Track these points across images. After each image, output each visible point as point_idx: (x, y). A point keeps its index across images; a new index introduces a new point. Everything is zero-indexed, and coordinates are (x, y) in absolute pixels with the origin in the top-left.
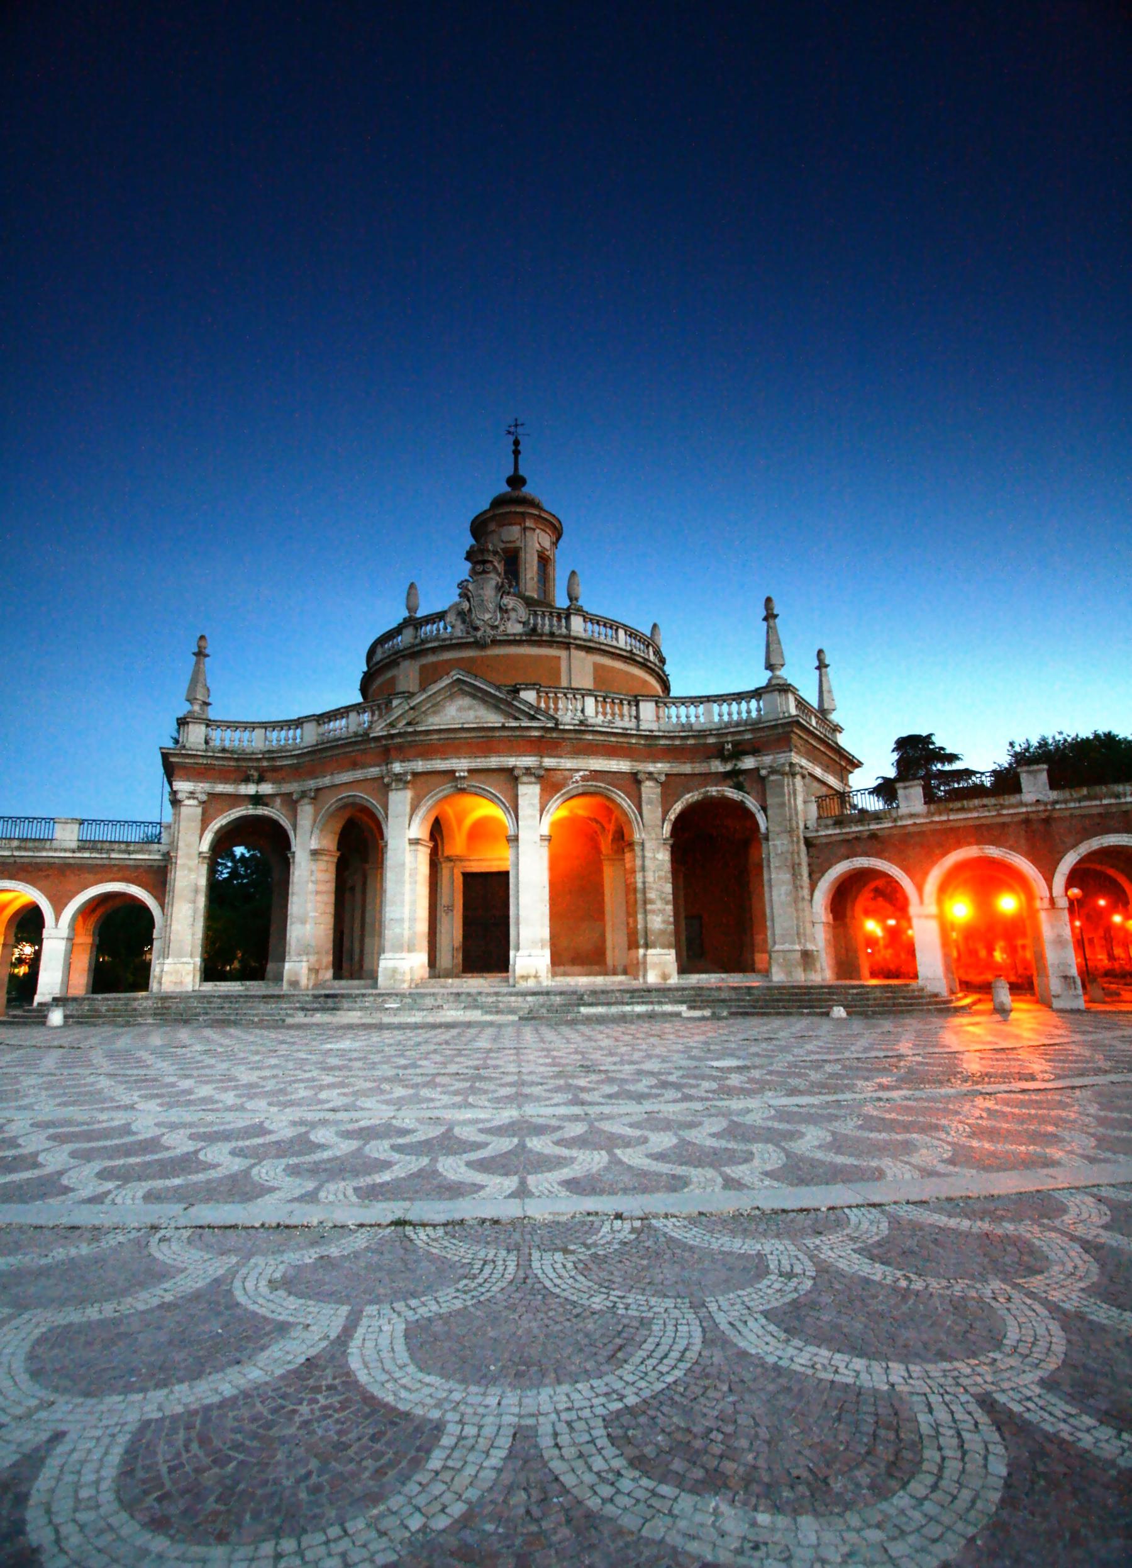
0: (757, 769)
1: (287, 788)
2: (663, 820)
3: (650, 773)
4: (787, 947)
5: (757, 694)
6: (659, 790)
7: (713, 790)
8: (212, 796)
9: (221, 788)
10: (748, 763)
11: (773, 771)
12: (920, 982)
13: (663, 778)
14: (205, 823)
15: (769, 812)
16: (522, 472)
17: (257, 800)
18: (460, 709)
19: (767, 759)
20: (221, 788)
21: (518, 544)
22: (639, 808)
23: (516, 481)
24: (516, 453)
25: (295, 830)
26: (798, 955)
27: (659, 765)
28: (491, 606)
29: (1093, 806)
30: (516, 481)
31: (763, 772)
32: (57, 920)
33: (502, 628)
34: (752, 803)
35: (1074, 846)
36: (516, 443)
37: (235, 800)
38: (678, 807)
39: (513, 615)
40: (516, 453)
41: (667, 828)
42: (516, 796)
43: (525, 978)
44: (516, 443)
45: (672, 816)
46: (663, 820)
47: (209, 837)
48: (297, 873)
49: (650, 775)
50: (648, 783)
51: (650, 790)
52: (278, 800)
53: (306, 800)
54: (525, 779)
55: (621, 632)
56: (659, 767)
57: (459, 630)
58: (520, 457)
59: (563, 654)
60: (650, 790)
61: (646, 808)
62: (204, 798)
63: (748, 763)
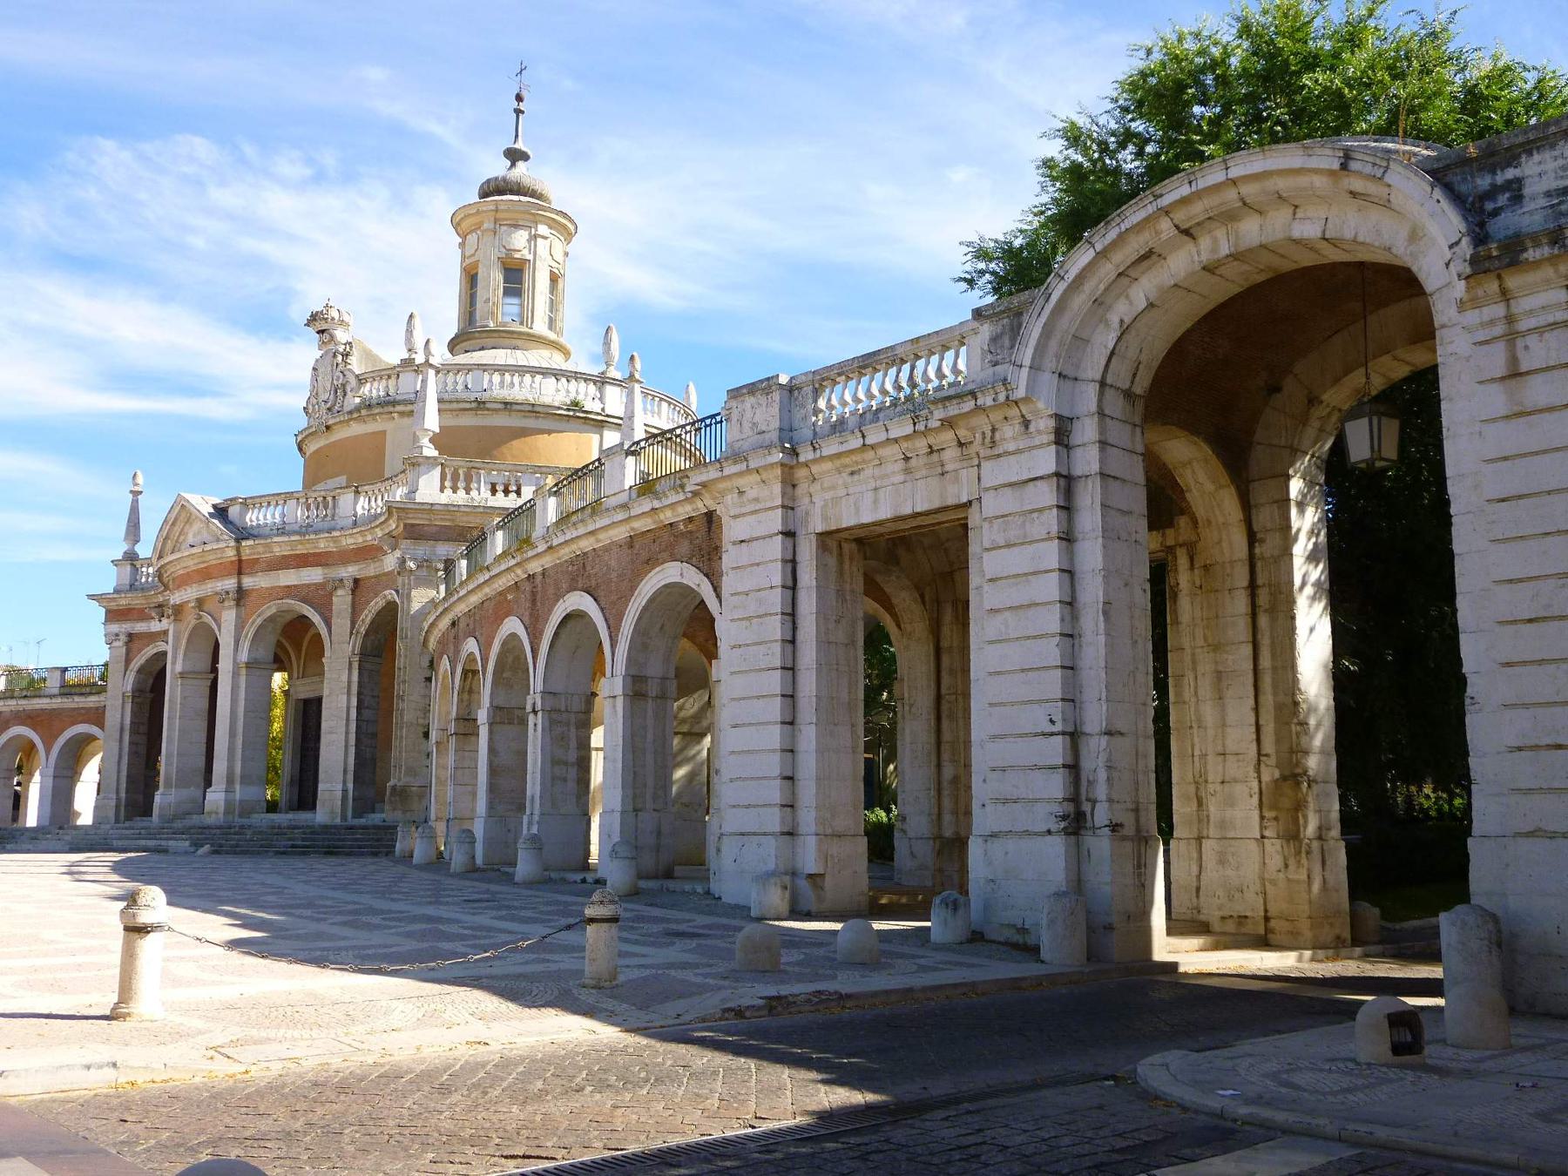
8: (130, 636)
14: (128, 661)
24: (518, 112)
27: (350, 569)
36: (519, 98)
38: (367, 616)
47: (131, 677)
50: (340, 592)
56: (349, 571)
62: (123, 638)
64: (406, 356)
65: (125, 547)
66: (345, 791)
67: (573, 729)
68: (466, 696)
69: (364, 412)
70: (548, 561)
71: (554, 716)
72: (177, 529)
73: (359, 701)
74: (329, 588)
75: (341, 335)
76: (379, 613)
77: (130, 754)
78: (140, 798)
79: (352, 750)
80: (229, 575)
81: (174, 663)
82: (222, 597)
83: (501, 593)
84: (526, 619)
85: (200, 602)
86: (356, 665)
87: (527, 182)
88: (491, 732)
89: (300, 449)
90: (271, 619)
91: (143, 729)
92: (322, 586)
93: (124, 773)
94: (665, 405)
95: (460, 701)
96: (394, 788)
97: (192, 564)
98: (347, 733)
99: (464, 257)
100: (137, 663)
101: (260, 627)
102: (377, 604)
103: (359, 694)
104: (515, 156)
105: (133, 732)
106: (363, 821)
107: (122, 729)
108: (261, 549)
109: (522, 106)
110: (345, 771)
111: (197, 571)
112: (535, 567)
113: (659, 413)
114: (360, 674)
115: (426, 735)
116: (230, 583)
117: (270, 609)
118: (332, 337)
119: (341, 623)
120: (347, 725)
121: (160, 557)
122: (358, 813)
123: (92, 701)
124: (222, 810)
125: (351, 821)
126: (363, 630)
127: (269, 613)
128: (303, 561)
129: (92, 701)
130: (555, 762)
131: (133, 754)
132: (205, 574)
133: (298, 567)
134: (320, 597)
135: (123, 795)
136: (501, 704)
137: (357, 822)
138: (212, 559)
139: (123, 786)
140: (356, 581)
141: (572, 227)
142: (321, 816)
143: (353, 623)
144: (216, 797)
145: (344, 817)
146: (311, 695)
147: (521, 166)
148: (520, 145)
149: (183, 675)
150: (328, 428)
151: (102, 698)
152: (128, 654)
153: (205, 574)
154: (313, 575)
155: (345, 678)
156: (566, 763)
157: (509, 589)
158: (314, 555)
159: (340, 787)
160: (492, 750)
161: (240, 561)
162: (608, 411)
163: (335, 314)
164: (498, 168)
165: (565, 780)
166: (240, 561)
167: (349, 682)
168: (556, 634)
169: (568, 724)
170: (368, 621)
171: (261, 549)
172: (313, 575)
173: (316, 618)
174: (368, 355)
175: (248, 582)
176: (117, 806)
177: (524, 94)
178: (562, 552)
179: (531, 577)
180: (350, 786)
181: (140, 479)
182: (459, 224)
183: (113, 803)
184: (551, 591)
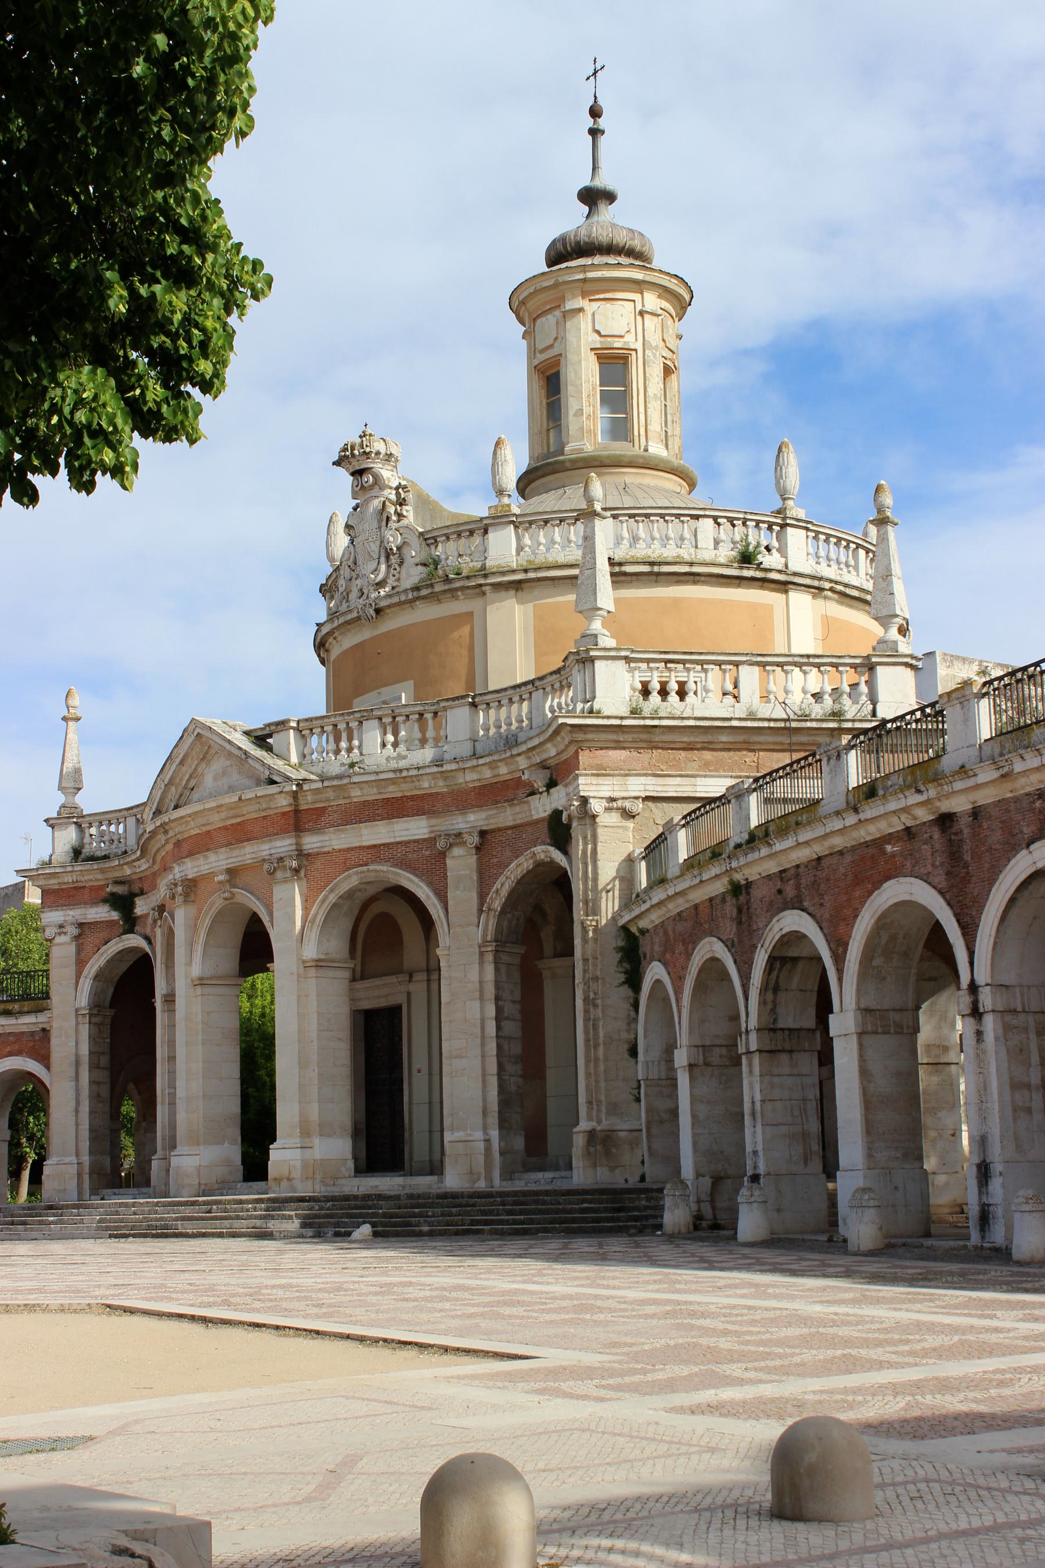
3: (459, 835)
8: (81, 925)
13: (476, 839)
14: (80, 963)
24: (595, 133)
27: (472, 817)
36: (595, 112)
38: (504, 885)
44: (595, 112)
46: (480, 911)
47: (86, 985)
50: (457, 851)
51: (461, 864)
58: (602, 140)
60: (461, 864)
61: (453, 895)
62: (72, 931)
64: (495, 502)
65: (61, 799)
66: (487, 1141)
67: (1033, 1037)
68: (770, 996)
70: (986, 797)
71: (1008, 1018)
72: (186, 770)
73: (499, 1010)
74: (440, 844)
75: (388, 475)
76: (519, 882)
77: (91, 1097)
78: (107, 1161)
79: (494, 1081)
80: (282, 832)
81: (189, 963)
83: (866, 844)
84: (940, 879)
85: (232, 872)
86: (490, 957)
87: (621, 239)
88: (861, 1046)
89: (321, 646)
90: (349, 895)
91: (104, 1061)
92: (431, 841)
93: (85, 1126)
94: (862, 553)
95: (763, 1003)
96: (591, 1134)
97: (216, 820)
98: (483, 1056)
99: (532, 351)
101: (335, 906)
102: (519, 867)
103: (497, 998)
104: (593, 197)
105: (94, 1066)
106: (519, 1185)
107: (78, 1063)
108: (330, 794)
109: (602, 123)
110: (485, 1113)
111: (225, 828)
112: (959, 805)
113: (856, 568)
114: (497, 970)
115: (633, 1052)
116: (283, 845)
117: (349, 880)
118: (377, 478)
119: (463, 895)
120: (483, 1045)
121: (158, 812)
122: (508, 1174)
123: (27, 1022)
124: (296, 1174)
125: (498, 1185)
126: (497, 905)
127: (346, 887)
128: (395, 808)
129: (27, 1022)
130: (1016, 1086)
131: (95, 1097)
132: (239, 833)
133: (390, 816)
134: (430, 858)
135: (86, 1159)
136: (873, 1005)
137: (509, 1187)
138: (251, 812)
139: (85, 1145)
140: (483, 834)
141: (687, 298)
142: (453, 1180)
143: (482, 897)
144: (281, 1156)
145: (489, 1179)
146: (383, 1003)
147: (607, 213)
148: (604, 181)
149: (201, 982)
150: (378, 611)
151: (42, 1018)
152: (79, 950)
153: (239, 833)
154: (414, 828)
155: (474, 975)
156: (1028, 1086)
157: (888, 838)
158: (412, 798)
159: (479, 1135)
160: (864, 1073)
161: (297, 811)
162: (793, 567)
163: (379, 446)
164: (571, 219)
165: (1029, 1111)
166: (297, 811)
167: (481, 982)
168: (1012, 901)
169: (1026, 1030)
170: (505, 892)
171: (330, 794)
172: (414, 828)
173: (423, 891)
174: (425, 503)
175: (311, 842)
176: (80, 1175)
177: (600, 102)
178: (1022, 781)
179: (945, 820)
180: (495, 1134)
181: (75, 701)
182: (523, 303)
183: (73, 1170)
184: (996, 837)
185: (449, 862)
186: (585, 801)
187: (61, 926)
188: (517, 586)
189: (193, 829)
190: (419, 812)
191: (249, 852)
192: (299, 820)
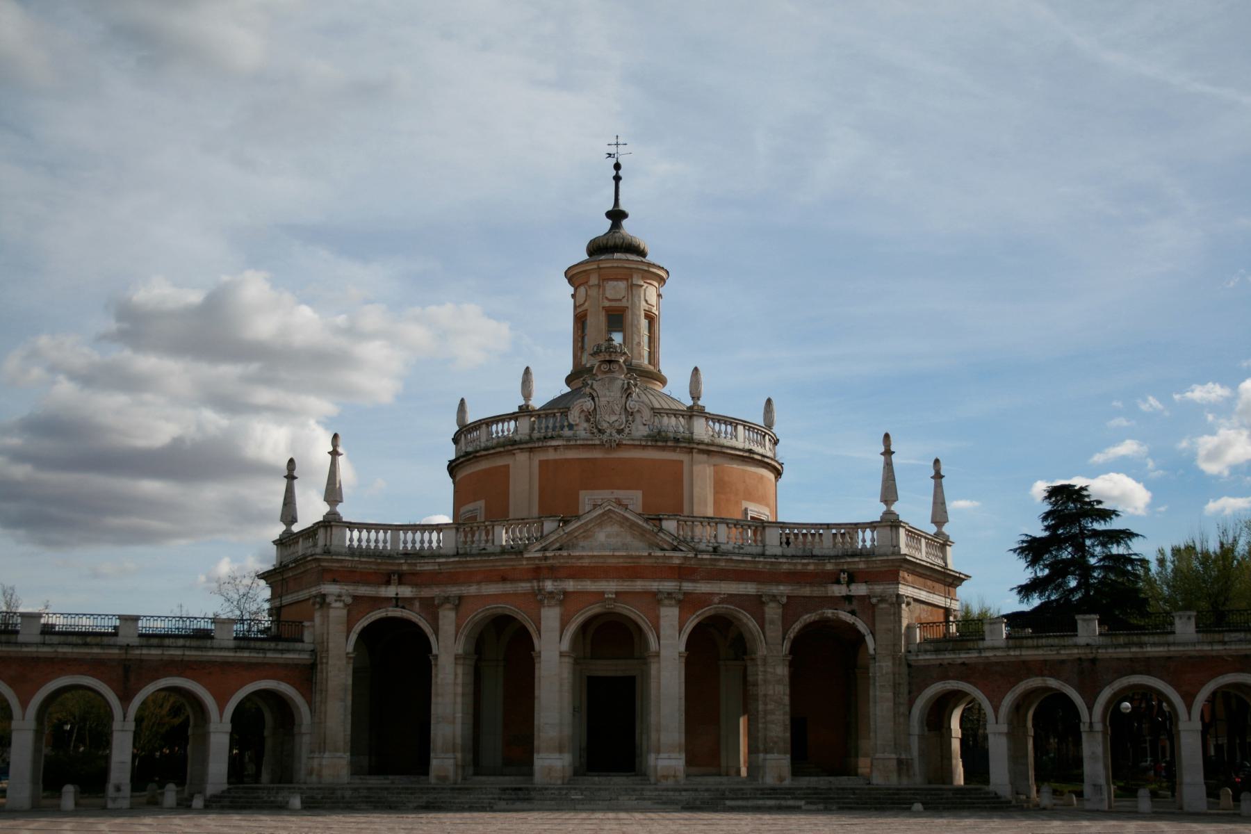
0: (869, 597)
1: (426, 593)
2: (784, 639)
3: (774, 596)
4: (887, 755)
5: (872, 526)
6: (780, 611)
7: (829, 613)
8: (356, 598)
9: (363, 590)
10: (860, 589)
11: (882, 599)
12: (991, 788)
13: (784, 600)
15: (877, 637)
16: (623, 206)
17: (398, 601)
18: (608, 536)
19: (878, 589)
20: (363, 590)
21: (624, 303)
22: (762, 628)
23: (616, 216)
24: (617, 179)
25: (436, 632)
26: (895, 762)
27: (782, 588)
28: (617, 409)
29: (1125, 653)
30: (616, 216)
31: (874, 600)
32: (221, 716)
33: (627, 431)
34: (862, 627)
35: (1110, 683)
36: (617, 166)
37: (377, 602)
38: (797, 626)
39: (638, 417)
40: (617, 179)
41: (787, 645)
42: (658, 617)
43: (666, 777)
44: (617, 166)
45: (792, 634)
46: (784, 639)
47: (353, 637)
48: (440, 676)
49: (774, 598)
50: (772, 605)
51: (773, 612)
52: (417, 604)
53: (448, 606)
54: (666, 602)
55: (740, 428)
56: (783, 589)
57: (583, 430)
58: (621, 183)
59: (685, 458)
60: (773, 612)
62: (349, 600)
63: (860, 589)
69: (670, 444)
82: (656, 599)
100: (358, 628)
116: (669, 586)
119: (774, 631)
126: (792, 636)
134: (756, 604)
154: (750, 588)
172: (750, 588)
175: (688, 586)
185: (767, 609)
186: (898, 596)
187: (340, 596)
188: (708, 452)
189: (586, 562)
190: (751, 580)
191: (639, 585)
192: (682, 573)
